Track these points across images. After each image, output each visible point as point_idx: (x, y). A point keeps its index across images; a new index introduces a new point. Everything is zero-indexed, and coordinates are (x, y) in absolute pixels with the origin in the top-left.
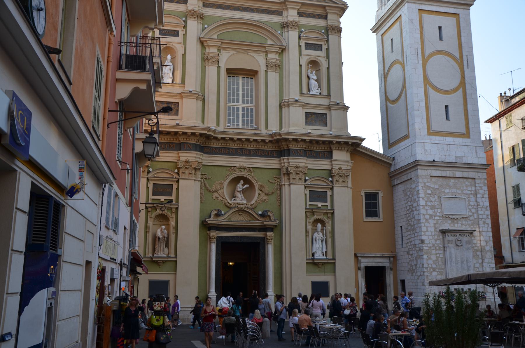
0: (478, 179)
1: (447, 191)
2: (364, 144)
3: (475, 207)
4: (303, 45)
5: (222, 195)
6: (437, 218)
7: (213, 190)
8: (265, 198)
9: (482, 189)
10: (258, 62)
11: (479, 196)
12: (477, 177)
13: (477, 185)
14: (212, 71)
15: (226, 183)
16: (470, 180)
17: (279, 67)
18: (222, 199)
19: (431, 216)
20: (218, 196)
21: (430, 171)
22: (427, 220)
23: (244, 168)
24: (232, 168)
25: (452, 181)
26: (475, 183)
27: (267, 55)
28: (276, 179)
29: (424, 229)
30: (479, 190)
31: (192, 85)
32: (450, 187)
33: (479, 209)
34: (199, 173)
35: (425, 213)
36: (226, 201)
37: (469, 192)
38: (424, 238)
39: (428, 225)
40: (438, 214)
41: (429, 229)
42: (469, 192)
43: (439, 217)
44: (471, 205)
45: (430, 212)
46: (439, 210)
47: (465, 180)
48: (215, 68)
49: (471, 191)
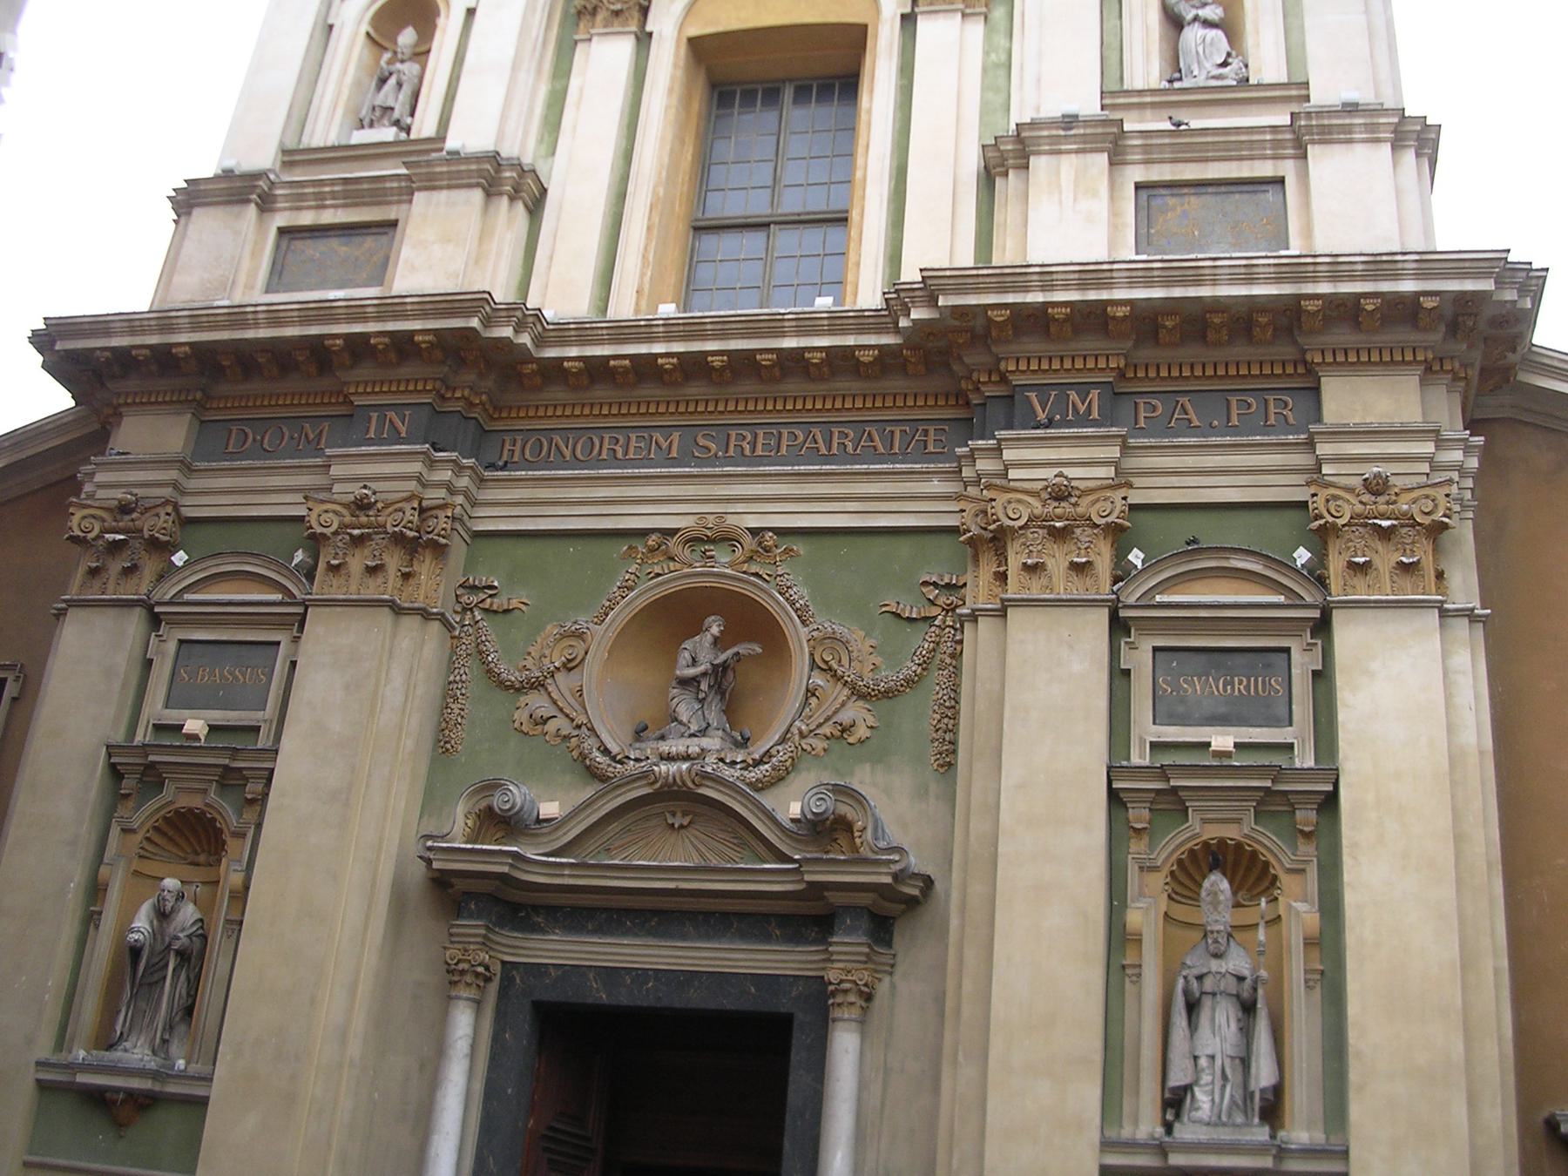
5: (568, 702)
7: (514, 676)
8: (845, 717)
14: (606, 58)
15: (602, 636)
18: (567, 729)
20: (546, 709)
23: (727, 538)
24: (652, 540)
28: (932, 593)
31: (470, 134)
34: (433, 584)
36: (590, 743)
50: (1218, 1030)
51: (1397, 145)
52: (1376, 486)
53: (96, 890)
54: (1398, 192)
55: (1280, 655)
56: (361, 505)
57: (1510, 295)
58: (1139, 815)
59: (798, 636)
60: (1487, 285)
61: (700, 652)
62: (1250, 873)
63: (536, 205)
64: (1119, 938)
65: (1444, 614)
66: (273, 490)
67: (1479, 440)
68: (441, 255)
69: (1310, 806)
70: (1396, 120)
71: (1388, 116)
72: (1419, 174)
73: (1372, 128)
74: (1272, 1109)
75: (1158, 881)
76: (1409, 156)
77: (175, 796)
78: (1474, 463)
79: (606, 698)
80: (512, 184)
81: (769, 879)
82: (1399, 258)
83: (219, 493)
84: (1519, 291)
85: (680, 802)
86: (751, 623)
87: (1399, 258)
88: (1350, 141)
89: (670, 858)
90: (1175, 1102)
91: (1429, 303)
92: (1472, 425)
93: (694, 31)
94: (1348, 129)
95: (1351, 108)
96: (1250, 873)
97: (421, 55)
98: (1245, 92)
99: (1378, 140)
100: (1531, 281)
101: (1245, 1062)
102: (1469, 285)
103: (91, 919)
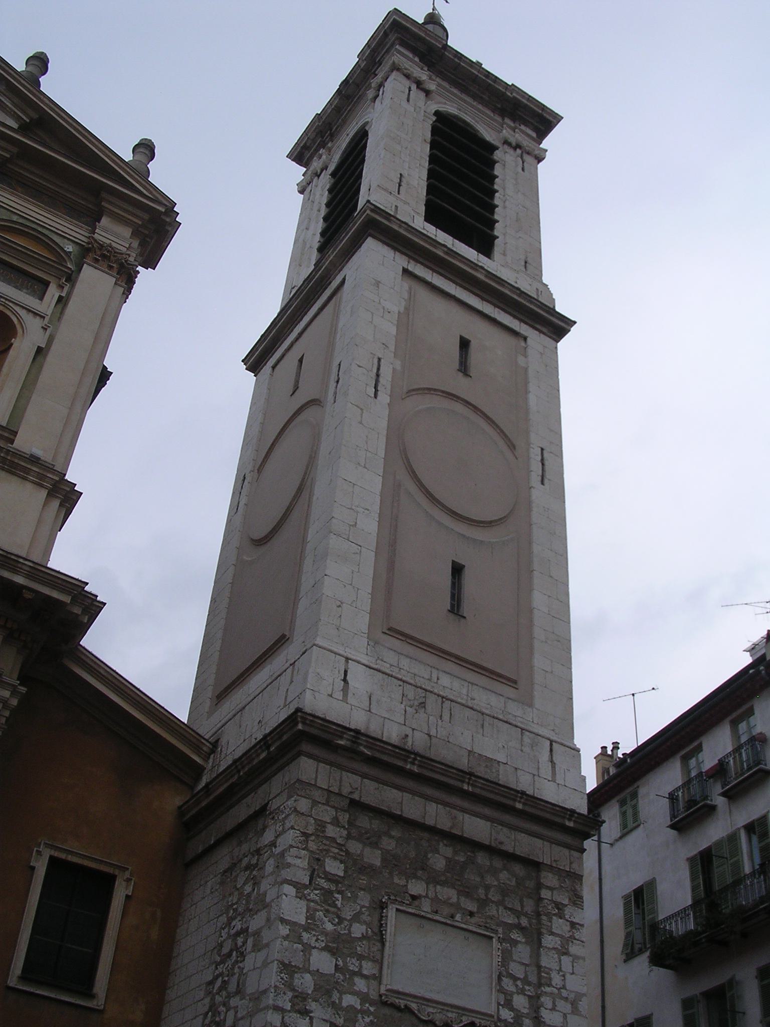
1: (416, 888)
2: (97, 641)
3: (530, 990)
6: (349, 1000)
9: (561, 916)
11: (548, 941)
12: (547, 861)
13: (545, 894)
16: (518, 869)
21: (355, 780)
22: (300, 998)
25: (446, 850)
26: (539, 886)
30: (549, 916)
32: (433, 879)
33: (546, 1001)
35: (298, 961)
37: (511, 919)
42: (511, 919)
43: (364, 998)
44: (515, 979)
46: (368, 968)
47: (498, 863)
49: (518, 914)
51: (51, 494)
54: (39, 521)
57: (77, 610)
60: (66, 599)
67: (23, 689)
70: (57, 479)
71: (53, 474)
72: (57, 516)
73: (42, 477)
76: (55, 504)
78: (14, 702)
82: (21, 560)
84: (84, 610)
87: (21, 560)
88: (25, 479)
91: (28, 595)
92: (23, 679)
94: (27, 471)
95: (34, 460)
99: (42, 486)
100: (92, 607)
102: (55, 595)
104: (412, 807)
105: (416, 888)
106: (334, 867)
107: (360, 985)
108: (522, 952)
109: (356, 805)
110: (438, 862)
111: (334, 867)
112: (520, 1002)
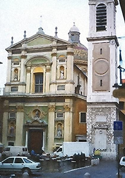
0: (112, 108)
1: (98, 113)
4: (58, 61)
6: (93, 123)
10: (43, 70)
14: (28, 74)
17: (49, 70)
19: (91, 123)
23: (37, 107)
27: (46, 67)
29: (87, 127)
31: (21, 81)
38: (87, 130)
39: (89, 126)
40: (94, 122)
41: (90, 127)
45: (91, 121)
46: (94, 120)
48: (30, 74)
50: (59, 131)
52: (67, 106)
53: (8, 126)
55: (61, 115)
56: (19, 106)
58: (56, 122)
59: (41, 112)
61: (37, 113)
62: (61, 125)
63: (26, 85)
64: (55, 128)
65: (70, 112)
66: (14, 105)
68: (21, 90)
69: (63, 121)
74: (61, 135)
75: (57, 124)
77: (12, 122)
79: (32, 115)
80: (24, 84)
81: (40, 125)
83: (11, 105)
85: (36, 121)
86: (39, 111)
89: (35, 124)
90: (57, 135)
93: (34, 72)
96: (61, 125)
97: (17, 73)
98: (64, 79)
101: (60, 133)
103: (8, 128)
104: (97, 107)
105: (98, 113)
106: (91, 114)
107: (94, 122)
108: (109, 115)
109: (92, 108)
110: (100, 110)
111: (91, 114)
112: (109, 120)
